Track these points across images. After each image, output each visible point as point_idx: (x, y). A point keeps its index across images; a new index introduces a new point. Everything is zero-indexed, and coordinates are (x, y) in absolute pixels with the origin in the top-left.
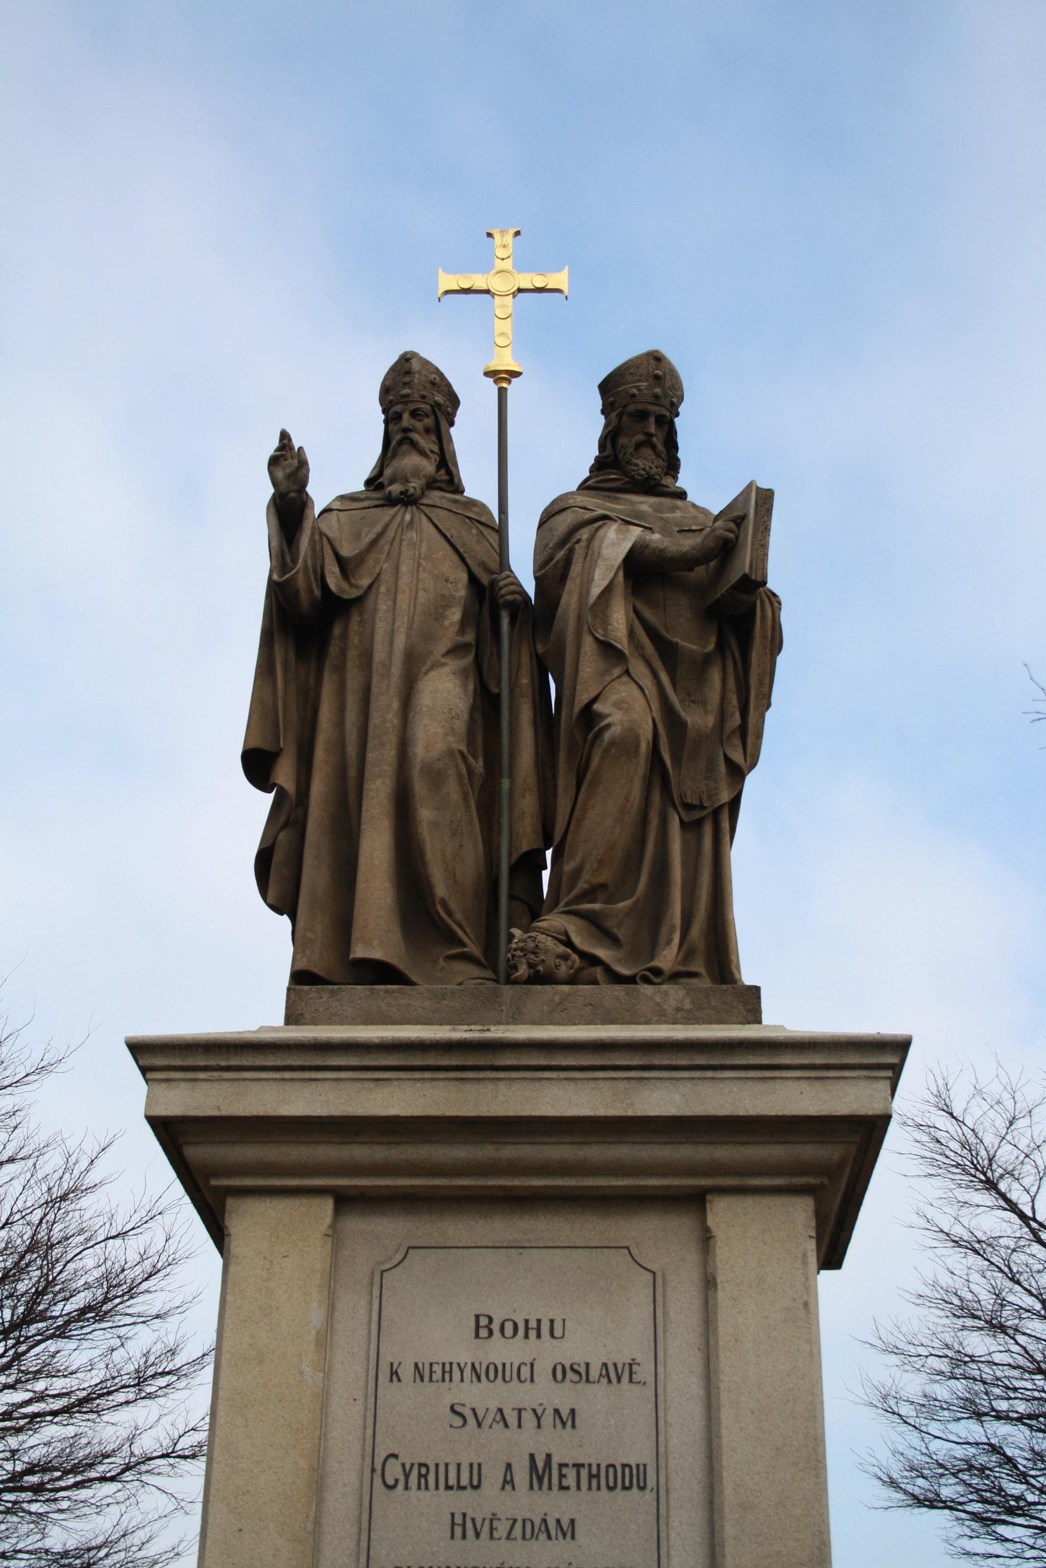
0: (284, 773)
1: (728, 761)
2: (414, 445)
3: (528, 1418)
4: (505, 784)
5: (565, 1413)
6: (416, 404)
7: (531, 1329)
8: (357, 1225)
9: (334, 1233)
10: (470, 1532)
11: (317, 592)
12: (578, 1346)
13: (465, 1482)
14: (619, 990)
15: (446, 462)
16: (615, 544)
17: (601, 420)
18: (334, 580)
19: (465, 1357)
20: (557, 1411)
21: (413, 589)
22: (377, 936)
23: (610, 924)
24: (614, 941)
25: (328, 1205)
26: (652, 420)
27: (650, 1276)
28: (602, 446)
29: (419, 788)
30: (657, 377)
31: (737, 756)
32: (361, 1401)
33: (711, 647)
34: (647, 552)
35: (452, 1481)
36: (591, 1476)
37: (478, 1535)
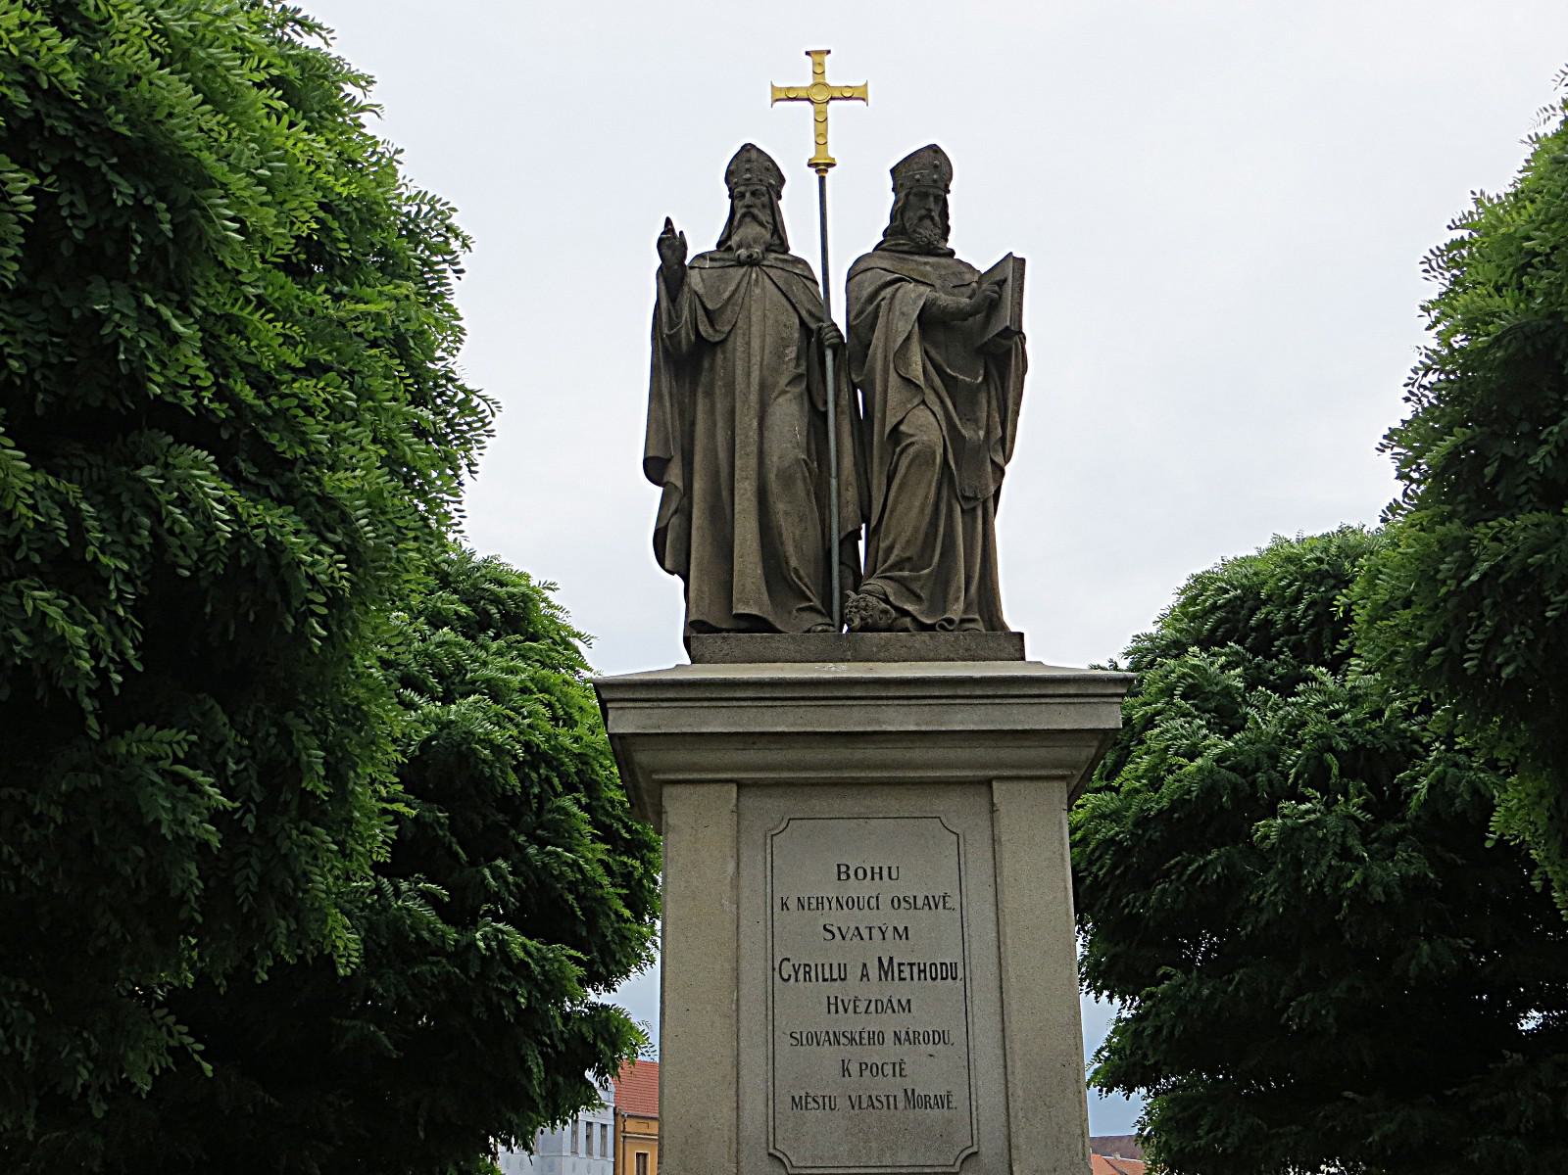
0: (674, 475)
1: (993, 462)
2: (755, 218)
3: (876, 933)
4: (834, 482)
5: (901, 930)
6: (753, 181)
7: (876, 874)
8: (750, 802)
9: (738, 811)
10: (841, 1008)
11: (693, 338)
12: (908, 886)
13: (835, 976)
14: (925, 636)
16: (912, 298)
17: (892, 197)
18: (704, 329)
19: (832, 895)
20: (895, 928)
21: (760, 336)
22: (751, 595)
23: (916, 587)
24: (918, 599)
25: (734, 788)
26: (932, 199)
27: (955, 837)
28: (893, 218)
29: (774, 486)
30: (936, 166)
31: (999, 459)
32: (762, 923)
33: (980, 379)
34: (934, 309)
35: (827, 976)
36: (920, 971)
37: (846, 1010)
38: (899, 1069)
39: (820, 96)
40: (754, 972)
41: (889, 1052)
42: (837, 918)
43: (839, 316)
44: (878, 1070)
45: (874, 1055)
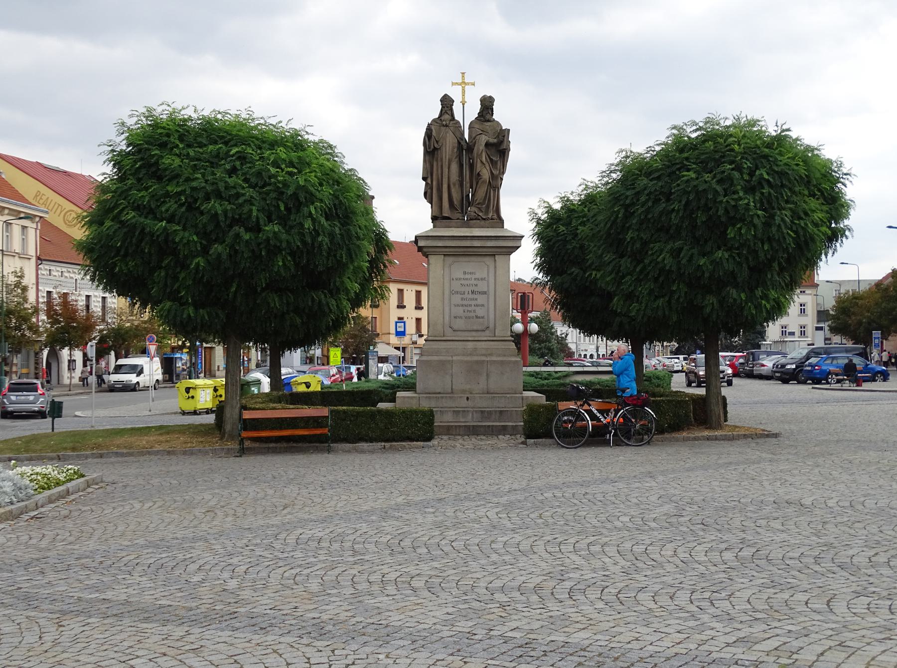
6: (447, 103)
7: (471, 273)
8: (447, 258)
15: (452, 115)
16: (484, 139)
18: (436, 146)
29: (452, 186)
38: (475, 311)
39: (464, 83)
40: (447, 292)
41: (473, 308)
42: (463, 282)
43: (466, 137)
44: (470, 311)
45: (470, 309)
